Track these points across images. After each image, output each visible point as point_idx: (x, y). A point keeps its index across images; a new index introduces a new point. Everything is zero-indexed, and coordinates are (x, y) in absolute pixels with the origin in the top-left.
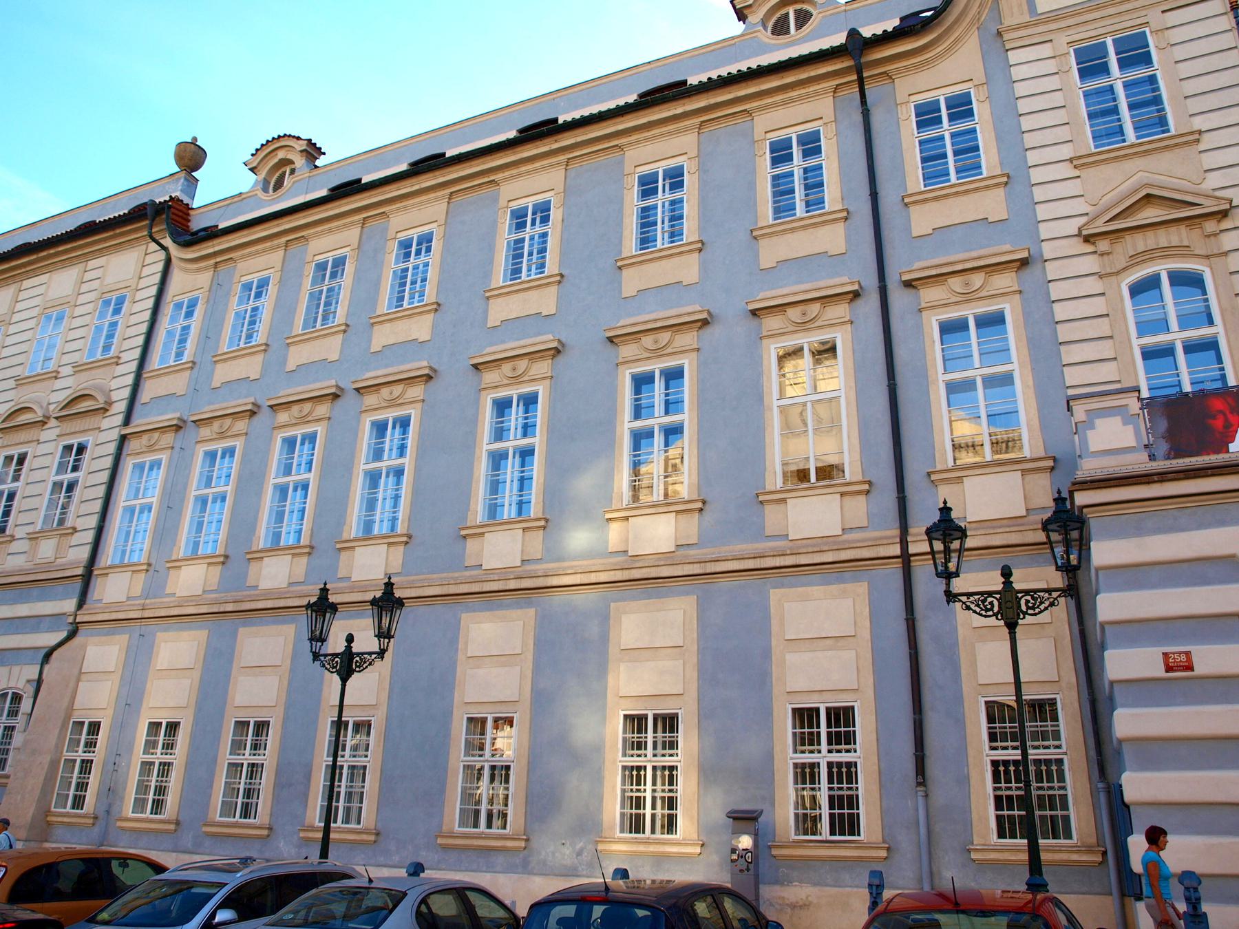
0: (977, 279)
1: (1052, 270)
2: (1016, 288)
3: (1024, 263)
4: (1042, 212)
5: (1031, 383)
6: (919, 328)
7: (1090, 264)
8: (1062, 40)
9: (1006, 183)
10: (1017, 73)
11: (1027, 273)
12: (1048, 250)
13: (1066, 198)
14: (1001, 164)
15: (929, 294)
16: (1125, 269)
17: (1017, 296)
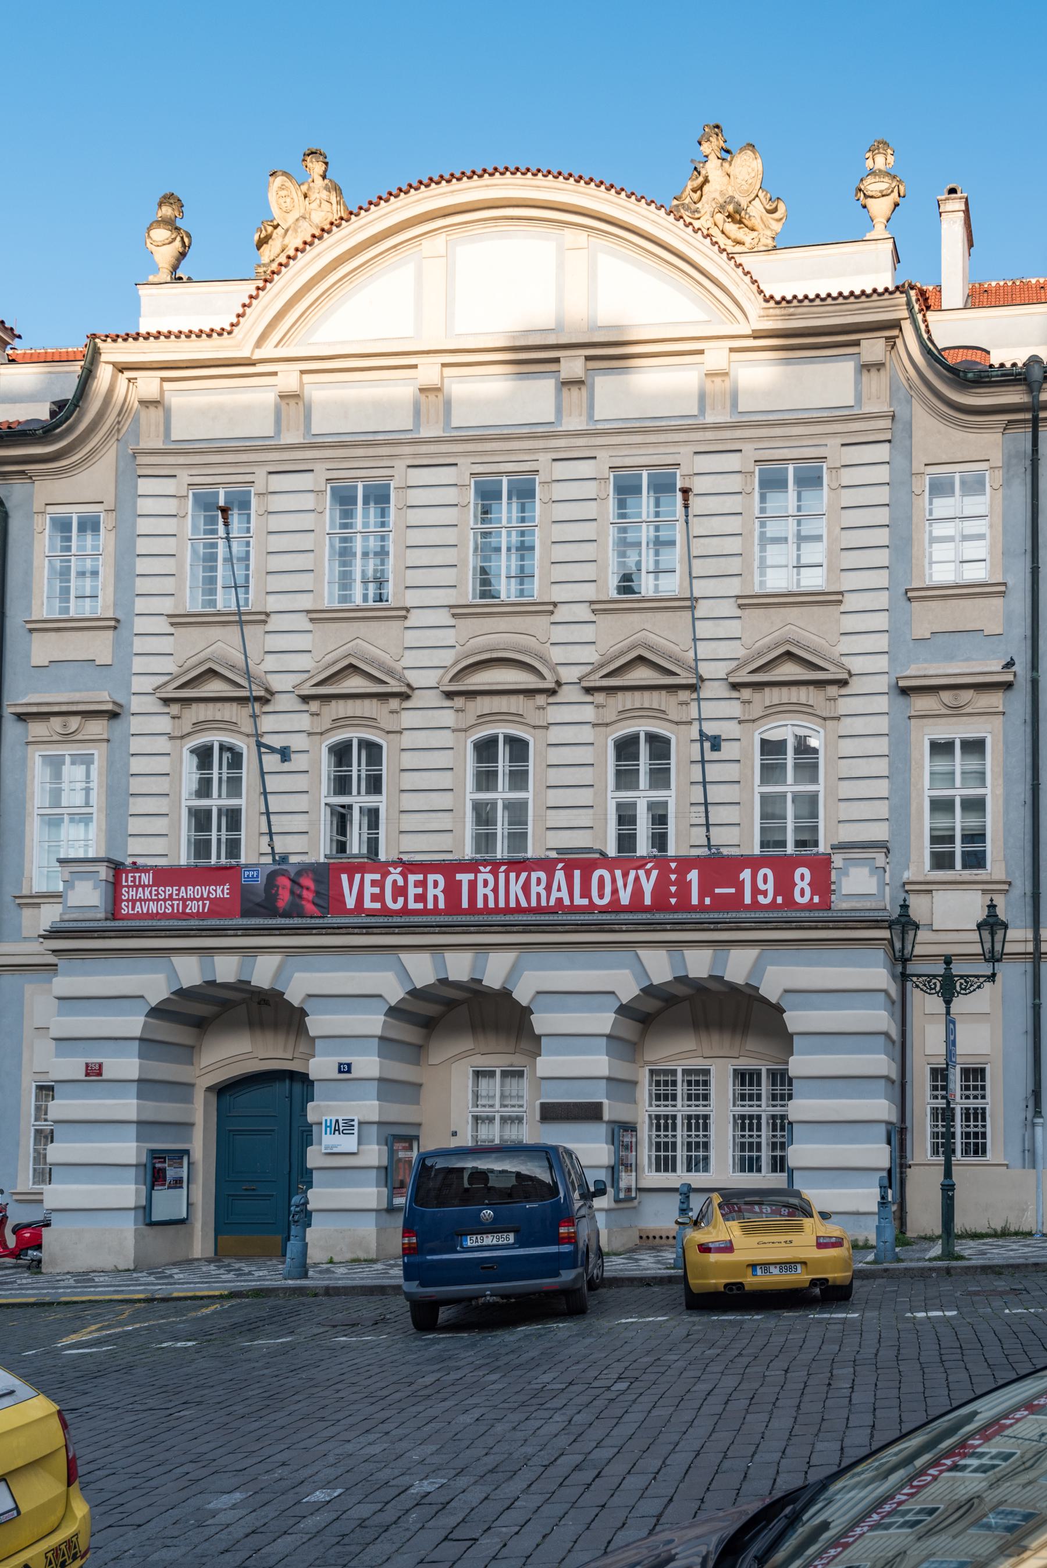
0: (74, 722)
1: (136, 724)
2: (105, 737)
3: (113, 715)
4: (138, 664)
5: (104, 827)
6: (23, 763)
7: (164, 724)
8: (185, 477)
9: (115, 628)
10: (145, 506)
11: (116, 723)
12: (136, 704)
13: (160, 656)
14: (115, 605)
15: (37, 729)
16: (189, 734)
17: (105, 744)
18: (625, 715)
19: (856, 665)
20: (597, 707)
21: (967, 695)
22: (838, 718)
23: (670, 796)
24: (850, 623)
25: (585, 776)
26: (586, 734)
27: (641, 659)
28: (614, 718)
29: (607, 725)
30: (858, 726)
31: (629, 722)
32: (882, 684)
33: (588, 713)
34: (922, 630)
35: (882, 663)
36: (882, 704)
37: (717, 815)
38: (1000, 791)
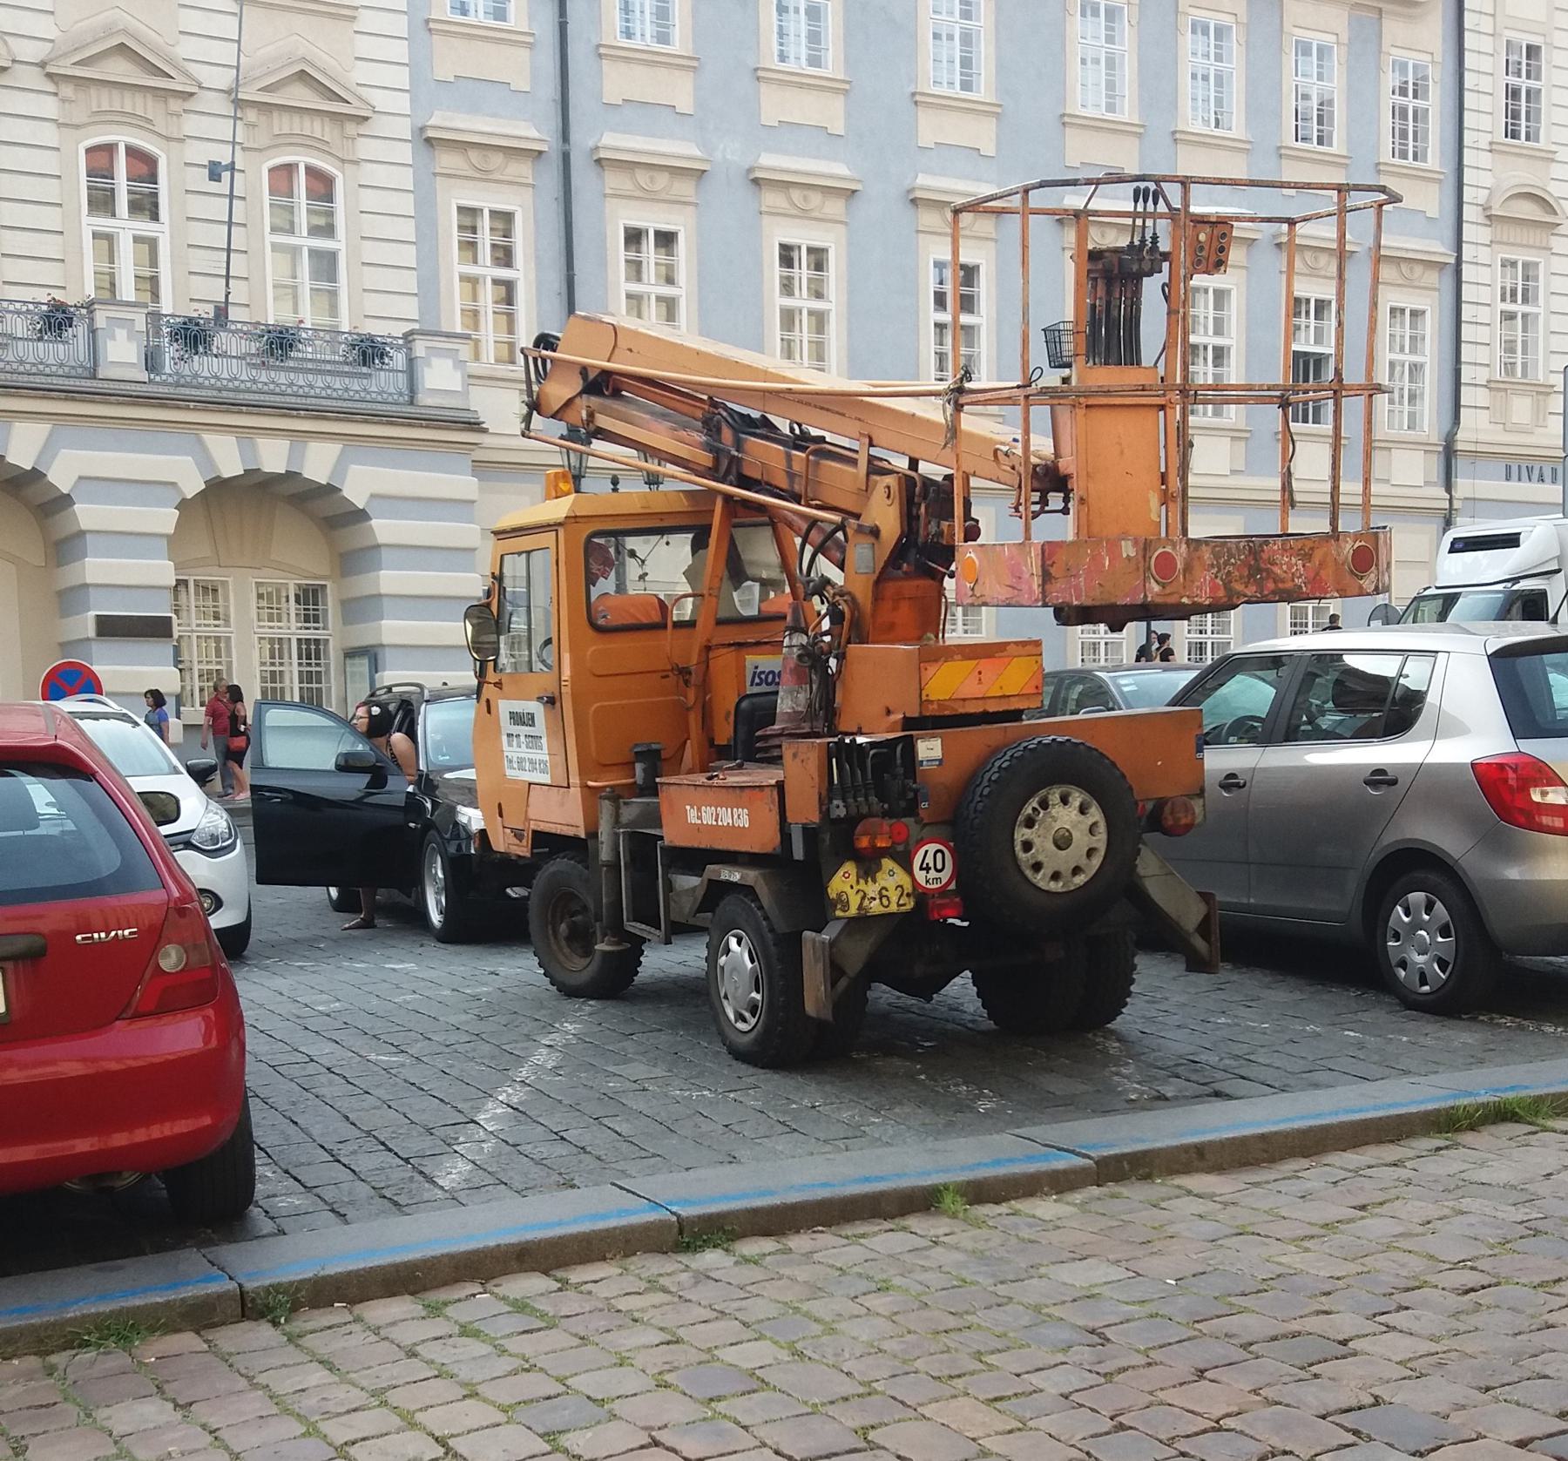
18: (103, 118)
19: (380, 100)
20: (63, 101)
21: (497, 159)
22: (356, 163)
23: (161, 231)
24: (365, 46)
25: (50, 191)
26: (49, 135)
27: (122, 48)
28: (85, 120)
29: (77, 127)
30: (378, 175)
31: (108, 127)
32: (404, 129)
33: (49, 107)
34: (444, 72)
35: (402, 103)
36: (405, 153)
37: (217, 263)
38: (532, 276)
